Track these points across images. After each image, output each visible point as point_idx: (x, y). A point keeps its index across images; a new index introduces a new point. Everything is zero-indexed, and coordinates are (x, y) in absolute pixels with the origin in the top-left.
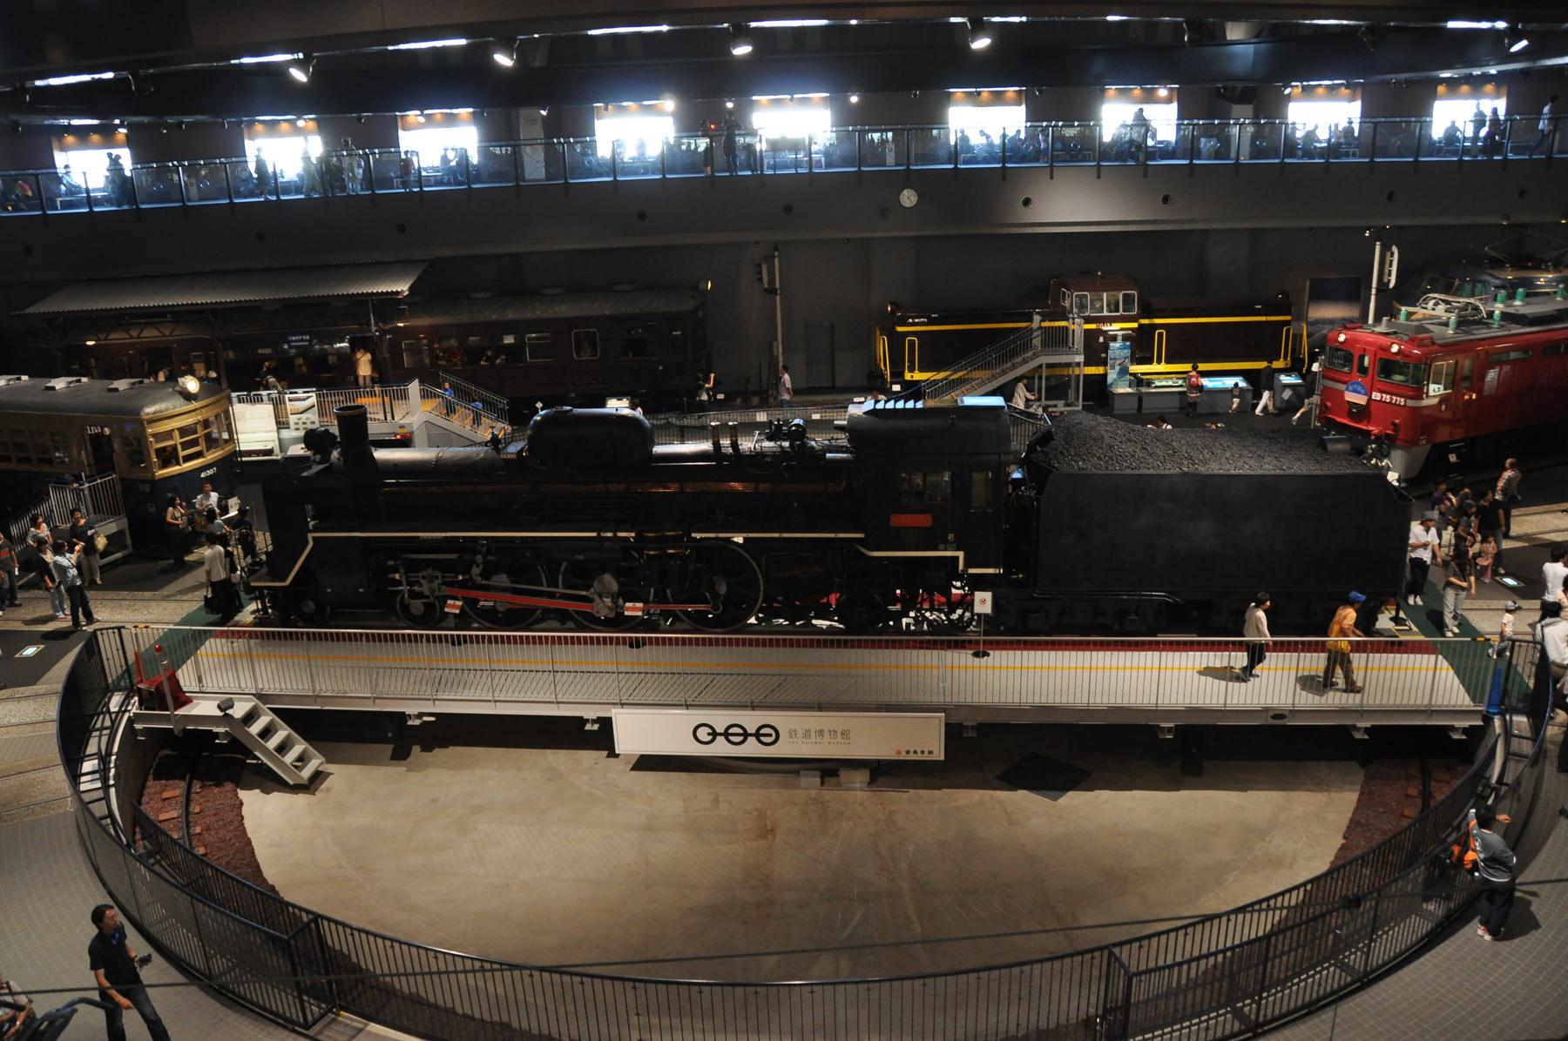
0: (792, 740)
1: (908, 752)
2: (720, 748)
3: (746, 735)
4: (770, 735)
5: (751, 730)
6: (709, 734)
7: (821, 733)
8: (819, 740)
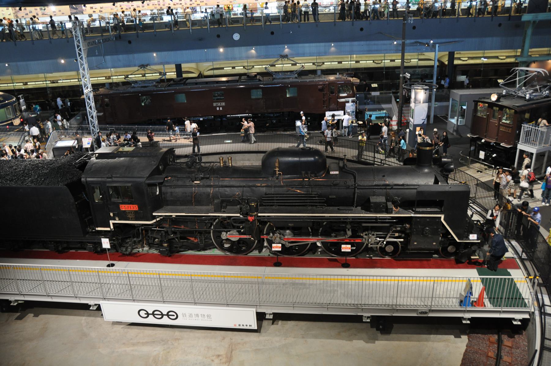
0: (184, 318)
2: (151, 320)
3: (163, 315)
6: (145, 314)
7: (197, 315)
8: (197, 318)
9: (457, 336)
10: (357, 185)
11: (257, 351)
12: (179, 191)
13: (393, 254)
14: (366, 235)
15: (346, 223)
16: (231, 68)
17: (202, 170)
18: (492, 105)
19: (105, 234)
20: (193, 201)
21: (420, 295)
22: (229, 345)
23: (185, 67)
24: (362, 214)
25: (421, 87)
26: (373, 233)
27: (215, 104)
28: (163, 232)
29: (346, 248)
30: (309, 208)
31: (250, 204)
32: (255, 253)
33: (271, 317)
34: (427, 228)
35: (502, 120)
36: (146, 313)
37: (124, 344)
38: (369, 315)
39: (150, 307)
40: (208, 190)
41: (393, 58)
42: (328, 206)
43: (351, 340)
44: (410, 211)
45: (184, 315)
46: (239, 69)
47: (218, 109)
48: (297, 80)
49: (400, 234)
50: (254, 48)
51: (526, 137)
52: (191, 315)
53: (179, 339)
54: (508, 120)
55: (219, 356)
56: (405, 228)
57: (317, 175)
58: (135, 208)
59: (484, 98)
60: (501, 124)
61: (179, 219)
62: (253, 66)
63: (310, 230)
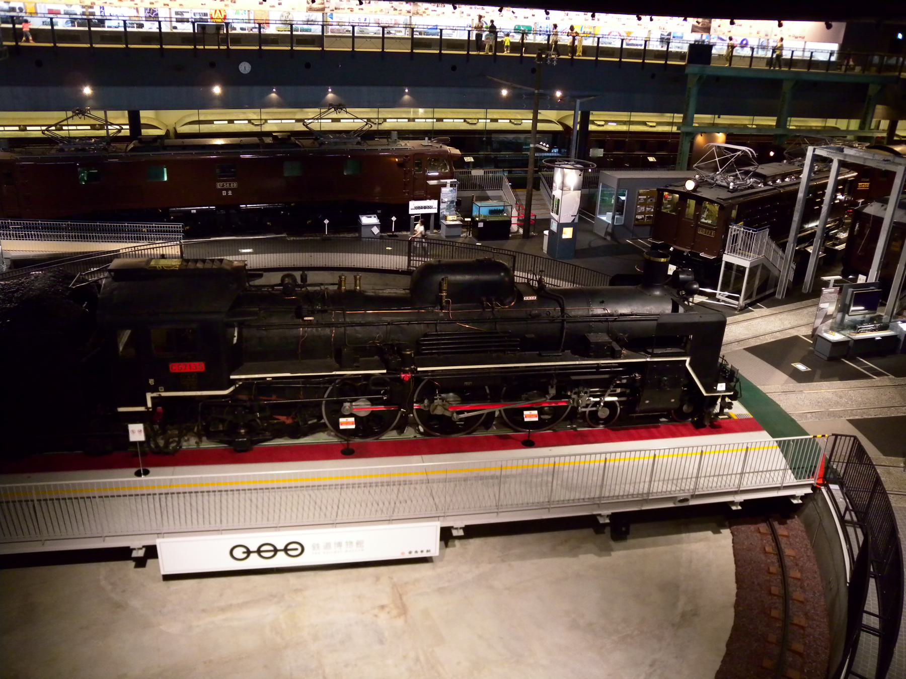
1: (410, 553)
2: (254, 562)
3: (276, 551)
4: (296, 549)
5: (280, 546)
6: (244, 553)
7: (339, 544)
9: (716, 531)
10: (567, 317)
11: (441, 590)
12: (274, 332)
13: (607, 421)
14: (575, 393)
15: (550, 377)
16: (226, 122)
17: (310, 298)
18: (685, 196)
19: (135, 418)
20: (300, 351)
21: (671, 477)
22: (393, 588)
23: (146, 116)
24: (578, 361)
25: (570, 164)
26: (586, 390)
27: (219, 185)
28: (240, 408)
29: (531, 416)
30: (494, 355)
31: (404, 352)
32: (391, 436)
33: (461, 533)
34: (665, 378)
35: (700, 219)
36: (245, 550)
37: (204, 611)
38: (609, 512)
39: (253, 541)
40: (327, 331)
41: (495, 117)
42: (522, 350)
43: (575, 555)
44: (643, 353)
45: (315, 547)
46: (241, 125)
47: (224, 193)
48: (359, 147)
49: (624, 390)
50: (274, 90)
51: (732, 244)
52: (328, 546)
53: (301, 590)
54: (709, 219)
55: (382, 607)
56: (634, 378)
57: (505, 302)
58: (199, 367)
59: (671, 186)
60: (699, 226)
61: (277, 383)
62: (266, 120)
63: (488, 391)
